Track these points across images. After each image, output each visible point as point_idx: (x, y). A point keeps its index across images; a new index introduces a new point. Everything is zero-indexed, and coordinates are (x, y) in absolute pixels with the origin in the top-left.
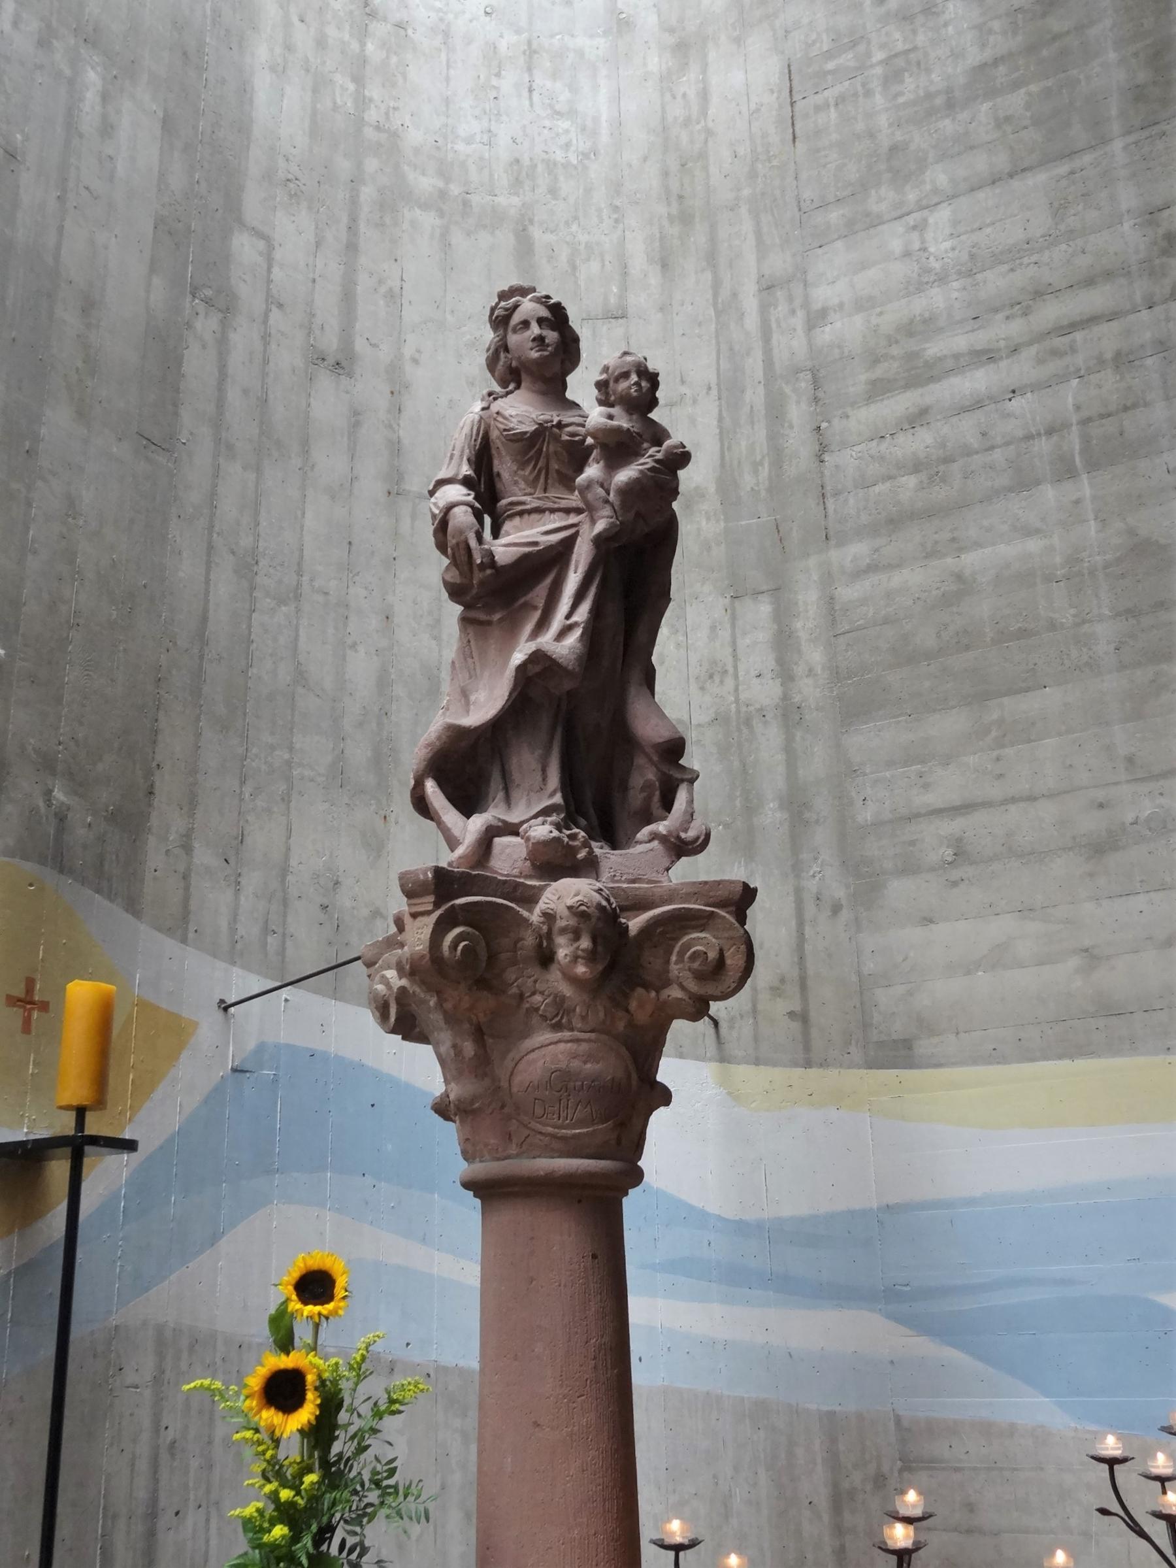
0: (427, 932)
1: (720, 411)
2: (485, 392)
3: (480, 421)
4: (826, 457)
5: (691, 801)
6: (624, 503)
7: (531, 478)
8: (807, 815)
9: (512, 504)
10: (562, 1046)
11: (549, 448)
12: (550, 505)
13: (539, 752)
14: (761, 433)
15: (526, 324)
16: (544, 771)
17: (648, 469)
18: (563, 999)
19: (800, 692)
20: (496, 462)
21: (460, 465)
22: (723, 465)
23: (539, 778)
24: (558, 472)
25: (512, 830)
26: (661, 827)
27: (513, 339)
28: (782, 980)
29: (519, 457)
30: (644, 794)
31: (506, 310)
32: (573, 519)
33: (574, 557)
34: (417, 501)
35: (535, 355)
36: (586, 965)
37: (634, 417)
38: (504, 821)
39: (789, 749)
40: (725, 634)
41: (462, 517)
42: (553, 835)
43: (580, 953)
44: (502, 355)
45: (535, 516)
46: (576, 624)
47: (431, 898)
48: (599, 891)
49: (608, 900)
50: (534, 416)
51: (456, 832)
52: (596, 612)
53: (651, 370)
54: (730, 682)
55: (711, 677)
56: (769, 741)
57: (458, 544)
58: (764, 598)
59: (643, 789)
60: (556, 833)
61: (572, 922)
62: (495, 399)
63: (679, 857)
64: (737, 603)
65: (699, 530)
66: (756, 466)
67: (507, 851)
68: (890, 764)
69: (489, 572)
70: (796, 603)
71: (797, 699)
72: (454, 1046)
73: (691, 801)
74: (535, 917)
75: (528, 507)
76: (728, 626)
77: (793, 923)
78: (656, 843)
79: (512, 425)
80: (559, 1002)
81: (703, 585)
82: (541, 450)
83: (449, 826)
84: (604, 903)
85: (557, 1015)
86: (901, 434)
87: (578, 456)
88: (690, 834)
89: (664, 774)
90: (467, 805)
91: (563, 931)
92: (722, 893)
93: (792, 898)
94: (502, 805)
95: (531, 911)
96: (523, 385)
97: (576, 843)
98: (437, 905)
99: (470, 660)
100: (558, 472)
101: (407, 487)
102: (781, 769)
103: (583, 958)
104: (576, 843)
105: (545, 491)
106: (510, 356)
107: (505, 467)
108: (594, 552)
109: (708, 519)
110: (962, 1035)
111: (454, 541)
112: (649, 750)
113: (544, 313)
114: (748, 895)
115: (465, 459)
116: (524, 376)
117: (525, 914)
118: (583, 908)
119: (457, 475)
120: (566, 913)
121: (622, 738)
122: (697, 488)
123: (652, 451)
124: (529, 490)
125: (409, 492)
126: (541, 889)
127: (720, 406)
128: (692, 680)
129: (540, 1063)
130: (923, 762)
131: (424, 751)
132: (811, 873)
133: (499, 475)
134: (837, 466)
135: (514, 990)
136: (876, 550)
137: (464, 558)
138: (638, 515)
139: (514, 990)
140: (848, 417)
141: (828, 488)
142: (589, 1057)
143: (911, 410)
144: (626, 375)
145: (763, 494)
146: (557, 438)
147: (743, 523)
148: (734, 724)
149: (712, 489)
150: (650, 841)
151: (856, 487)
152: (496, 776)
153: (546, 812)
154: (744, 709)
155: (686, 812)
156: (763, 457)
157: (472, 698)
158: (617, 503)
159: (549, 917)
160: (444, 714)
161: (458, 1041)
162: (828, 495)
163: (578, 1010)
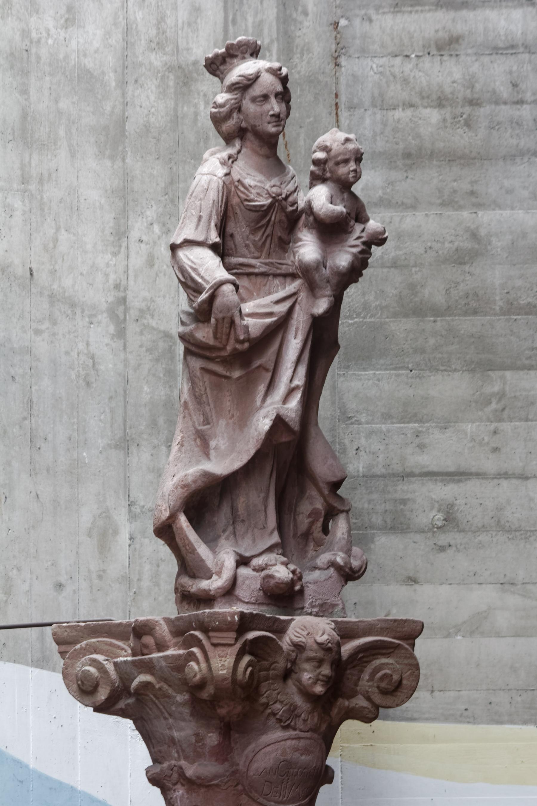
0: (230, 661)
3: (223, 187)
4: (343, 61)
7: (260, 243)
9: (242, 265)
10: (289, 742)
12: (274, 270)
13: (262, 495)
15: (265, 97)
18: (296, 707)
21: (208, 229)
29: (253, 224)
30: (311, 519)
31: (249, 80)
32: (292, 287)
36: (323, 686)
43: (321, 677)
44: (235, 115)
45: (259, 280)
46: (297, 388)
47: (233, 635)
50: (267, 187)
57: (224, 318)
59: (309, 516)
61: (320, 654)
65: (196, 114)
68: (387, 417)
72: (197, 735)
75: (256, 270)
78: (332, 570)
79: (252, 197)
80: (292, 710)
83: (204, 558)
85: (289, 719)
86: (427, 59)
91: (309, 660)
98: (237, 640)
103: (322, 681)
107: (240, 230)
110: (436, 694)
111: (220, 316)
112: (322, 485)
115: (213, 224)
118: (330, 645)
119: (207, 239)
120: (315, 646)
124: (257, 254)
129: (273, 756)
130: (421, 421)
131: (180, 490)
133: (232, 235)
134: (354, 76)
135: (263, 700)
136: (391, 183)
139: (263, 700)
140: (370, 20)
141: (343, 98)
142: (306, 751)
143: (441, 34)
144: (346, 161)
146: (283, 209)
151: (374, 106)
156: (272, 41)
157: (213, 443)
159: (299, 647)
161: (202, 731)
162: (342, 106)
163: (303, 715)
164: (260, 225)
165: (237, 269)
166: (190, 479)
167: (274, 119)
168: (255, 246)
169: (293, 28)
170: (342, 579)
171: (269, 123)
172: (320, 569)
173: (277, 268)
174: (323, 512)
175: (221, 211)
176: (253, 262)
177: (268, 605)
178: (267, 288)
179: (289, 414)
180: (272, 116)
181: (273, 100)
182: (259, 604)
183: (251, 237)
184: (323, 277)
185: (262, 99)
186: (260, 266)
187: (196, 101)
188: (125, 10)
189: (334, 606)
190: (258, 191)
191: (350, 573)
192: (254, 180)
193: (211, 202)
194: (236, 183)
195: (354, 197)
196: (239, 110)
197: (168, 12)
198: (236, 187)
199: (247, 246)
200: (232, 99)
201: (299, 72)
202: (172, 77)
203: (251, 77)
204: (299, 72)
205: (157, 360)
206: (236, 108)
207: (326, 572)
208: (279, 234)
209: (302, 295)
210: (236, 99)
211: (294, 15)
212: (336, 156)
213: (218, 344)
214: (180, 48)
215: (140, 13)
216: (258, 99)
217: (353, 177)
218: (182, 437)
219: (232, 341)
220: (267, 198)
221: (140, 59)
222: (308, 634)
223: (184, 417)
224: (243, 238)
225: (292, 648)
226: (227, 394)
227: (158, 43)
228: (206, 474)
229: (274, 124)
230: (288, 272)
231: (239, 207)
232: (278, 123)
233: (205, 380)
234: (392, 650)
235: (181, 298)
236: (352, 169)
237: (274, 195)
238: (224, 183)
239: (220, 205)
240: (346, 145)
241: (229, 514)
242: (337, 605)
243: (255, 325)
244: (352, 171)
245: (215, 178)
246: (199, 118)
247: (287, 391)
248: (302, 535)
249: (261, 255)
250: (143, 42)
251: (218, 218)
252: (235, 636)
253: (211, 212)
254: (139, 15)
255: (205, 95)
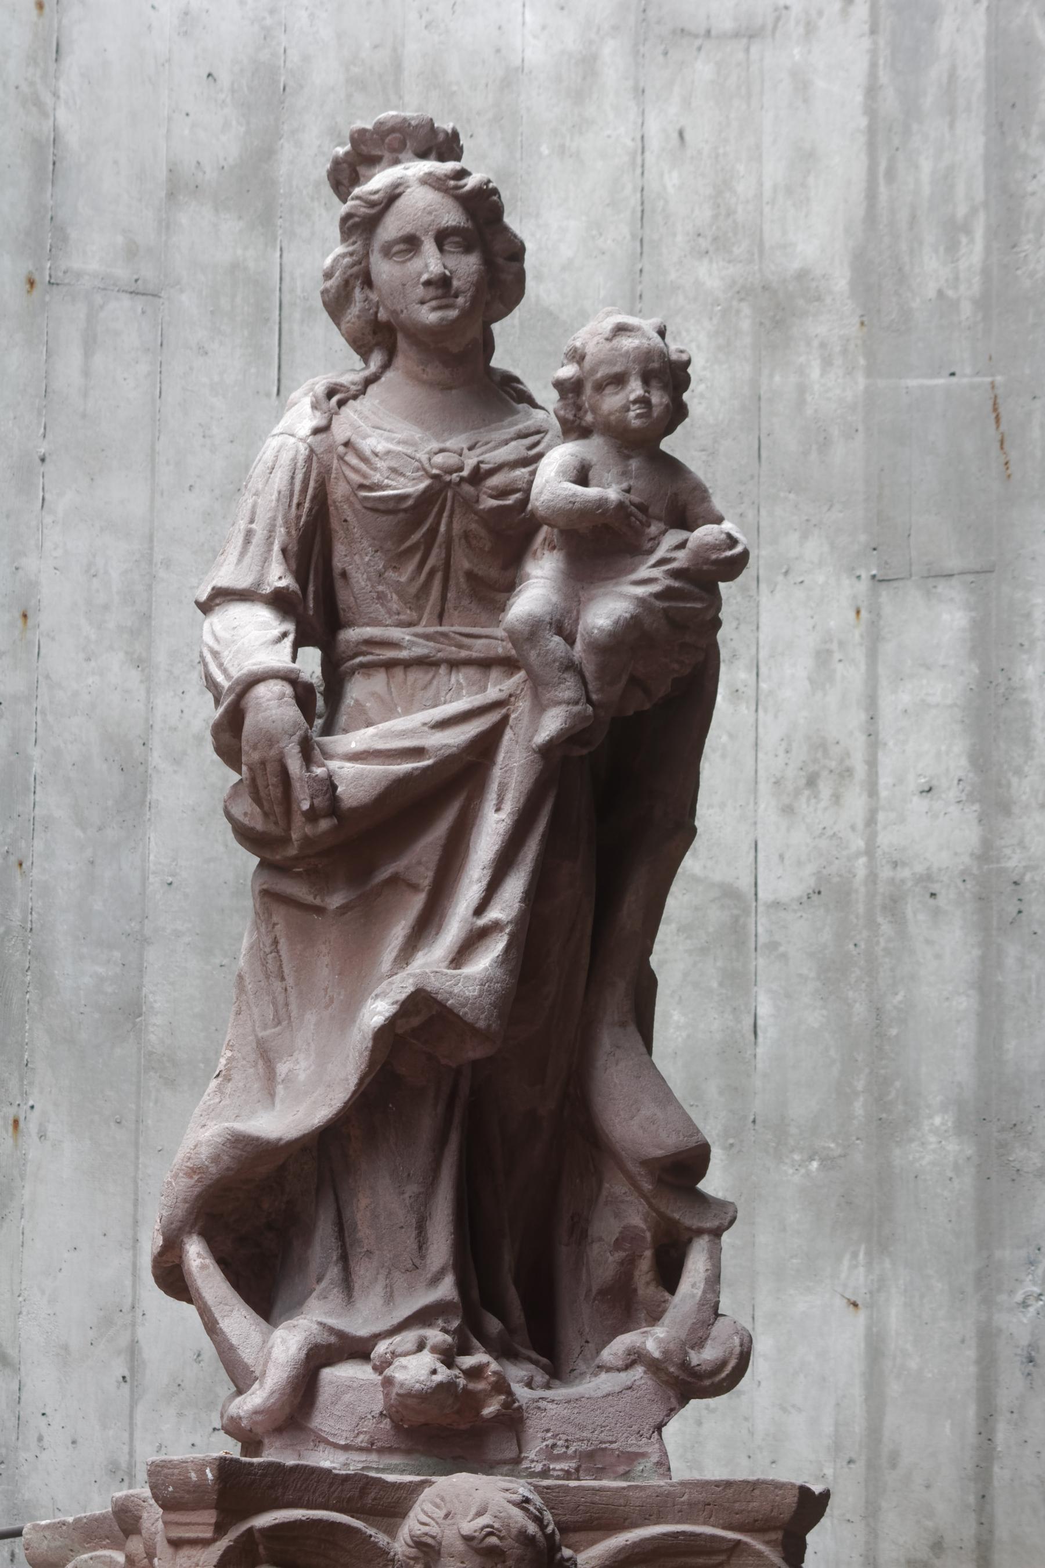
1: (873, 65)
2: (320, 389)
3: (309, 460)
5: (714, 1280)
6: (602, 669)
7: (413, 590)
8: (1019, 1153)
9: (372, 643)
11: (452, 524)
12: (452, 652)
13: (412, 1189)
14: (971, 142)
15: (411, 243)
16: (421, 1229)
17: (657, 596)
19: (1021, 844)
20: (340, 550)
21: (265, 560)
22: (871, 218)
23: (411, 1243)
24: (470, 575)
25: (356, 1349)
26: (652, 1339)
27: (383, 270)
28: (938, 1546)
29: (389, 545)
30: (620, 1255)
31: (372, 204)
33: (497, 773)
34: (98, 299)
35: (429, 316)
37: (634, 464)
38: (341, 1335)
39: (986, 985)
40: (851, 674)
41: (273, 707)
42: (438, 1378)
44: (358, 294)
45: (417, 676)
46: (495, 927)
47: (210, 1516)
48: (523, 1503)
49: (539, 1520)
51: (247, 1354)
52: (536, 895)
53: (674, 357)
54: (856, 803)
55: (812, 782)
56: (941, 958)
57: (263, 763)
58: (953, 591)
59: (618, 1245)
60: (444, 1374)
62: (341, 403)
63: (683, 1401)
64: (885, 595)
65: (802, 389)
66: (954, 232)
67: (347, 1398)
69: (324, 824)
70: (1028, 615)
71: (1014, 861)
73: (714, 1280)
74: (400, 1546)
75: (404, 654)
76: (859, 654)
77: (971, 1411)
78: (639, 1371)
79: (377, 477)
81: (805, 536)
82: (434, 531)
83: (234, 1341)
84: (532, 1528)
87: (512, 534)
88: (707, 1355)
89: (661, 1214)
90: (265, 1297)
92: (757, 1505)
93: (971, 1353)
94: (336, 1295)
95: (392, 1532)
96: (399, 361)
97: (481, 1386)
98: (220, 1529)
99: (277, 985)
100: (470, 575)
101: (76, 264)
102: (966, 1034)
104: (481, 1386)
105: (440, 618)
106: (374, 297)
107: (357, 560)
108: (538, 767)
109: (827, 363)
111: (256, 756)
112: (631, 1167)
113: (452, 216)
114: (811, 1506)
115: (276, 548)
116: (402, 343)
117: (381, 1539)
118: (493, 1540)
119: (259, 584)
120: (460, 1546)
121: (577, 1137)
122: (802, 275)
123: (673, 537)
124: (407, 615)
125: (79, 275)
126: (415, 1489)
127: (874, 53)
128: (764, 787)
132: (1019, 1297)
133: (344, 574)
137: (276, 792)
138: (634, 681)
144: (619, 380)
145: (966, 309)
146: (469, 505)
147: (912, 383)
148: (861, 909)
149: (841, 282)
150: (627, 1367)
152: (324, 1231)
153: (423, 1317)
154: (885, 873)
155: (702, 1303)
156: (974, 211)
158: (589, 669)
160: (220, 1089)
164: (408, 544)
165: (364, 654)
166: (205, 1152)
167: (432, 292)
168: (401, 596)
169: (1019, 175)
170: (671, 1393)
171: (422, 303)
172: (609, 1369)
173: (460, 646)
174: (648, 1235)
175: (298, 517)
176: (396, 633)
177: (408, 1452)
178: (431, 692)
179: (456, 990)
180: (428, 283)
181: (429, 247)
182: (381, 1451)
183: (391, 574)
184: (550, 657)
185: (402, 247)
186: (413, 644)
187: (802, 359)
188: (639, 171)
189: (633, 1457)
190: (393, 464)
191: (683, 1376)
192: (388, 440)
193: (274, 497)
194: (341, 449)
195: (672, 467)
196: (368, 282)
197: (741, 168)
198: (341, 458)
199: (381, 597)
200: (343, 256)
201: (1032, 275)
202: (746, 309)
203: (375, 197)
204: (1032, 275)
205: (704, 951)
206: (356, 276)
207: (623, 1375)
208: (467, 565)
209: (522, 706)
210: (351, 254)
211: (1023, 147)
212: (593, 371)
213: (272, 829)
214: (767, 245)
215: (675, 174)
216: (396, 249)
217: (638, 416)
218: (230, 1060)
219: (298, 820)
220: (419, 479)
221: (673, 276)
222: (447, 1516)
223: (238, 1013)
224: (369, 579)
225: (413, 1552)
226: (324, 949)
227: (715, 239)
228: (240, 1142)
229: (434, 303)
230: (492, 654)
231: (351, 504)
232: (444, 301)
233: (275, 919)
234: (722, 1558)
235: (762, 806)
236: (632, 397)
237: (435, 471)
238: (312, 451)
239: (295, 501)
240: (614, 342)
241: (332, 1242)
242: (643, 1455)
243: (358, 777)
244: (635, 402)
245: (292, 440)
246: (809, 398)
247: (463, 935)
248: (602, 1292)
249: (420, 619)
250: (679, 238)
251: (288, 533)
252: (213, 1521)
253: (274, 519)
254: (672, 180)
255: (823, 345)
